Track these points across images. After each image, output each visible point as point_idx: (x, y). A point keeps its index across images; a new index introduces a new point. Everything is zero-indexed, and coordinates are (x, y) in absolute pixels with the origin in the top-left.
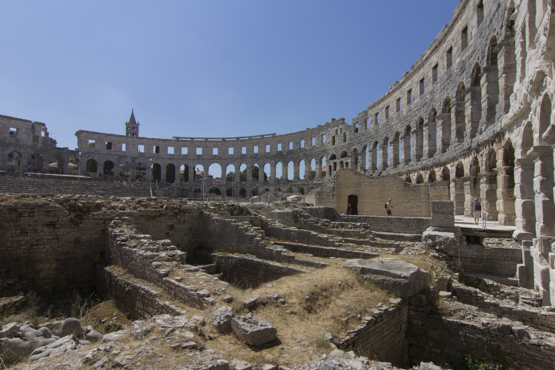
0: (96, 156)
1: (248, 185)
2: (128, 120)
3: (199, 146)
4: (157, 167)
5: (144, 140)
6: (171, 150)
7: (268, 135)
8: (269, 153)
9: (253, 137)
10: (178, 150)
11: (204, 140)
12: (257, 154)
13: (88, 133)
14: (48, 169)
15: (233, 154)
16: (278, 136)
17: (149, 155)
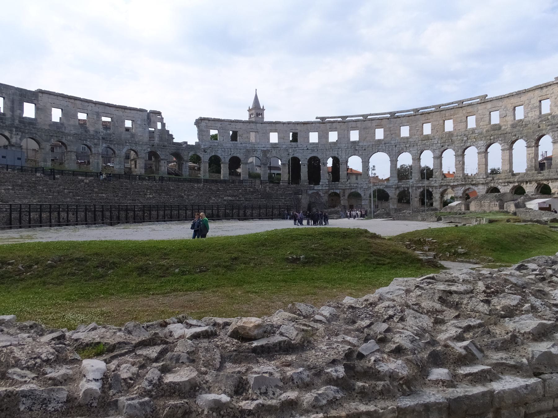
0: (219, 152)
1: (435, 185)
2: (251, 104)
3: (354, 129)
4: (295, 163)
5: (277, 125)
6: (314, 137)
7: (471, 99)
8: (473, 131)
9: (443, 105)
10: (323, 136)
11: (361, 118)
12: (450, 134)
13: (209, 120)
14: (166, 170)
15: (409, 136)
16: (491, 100)
17: (284, 146)
